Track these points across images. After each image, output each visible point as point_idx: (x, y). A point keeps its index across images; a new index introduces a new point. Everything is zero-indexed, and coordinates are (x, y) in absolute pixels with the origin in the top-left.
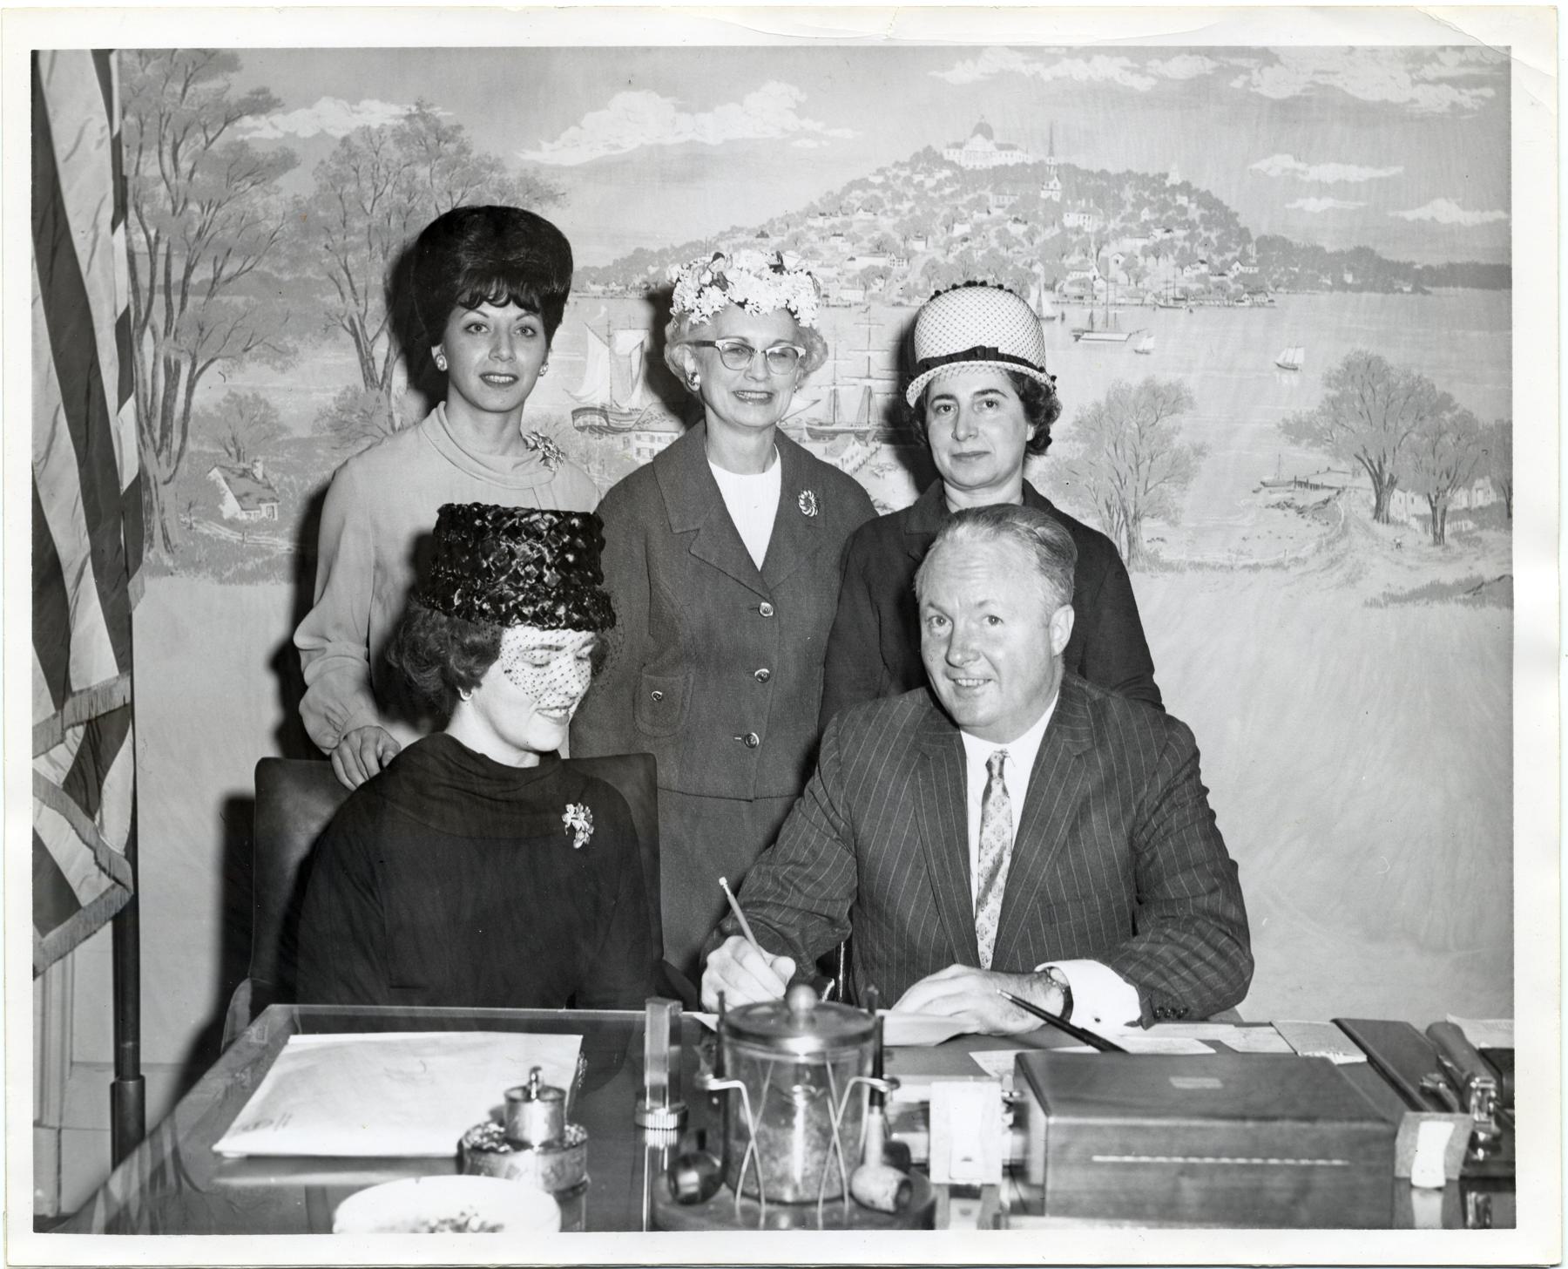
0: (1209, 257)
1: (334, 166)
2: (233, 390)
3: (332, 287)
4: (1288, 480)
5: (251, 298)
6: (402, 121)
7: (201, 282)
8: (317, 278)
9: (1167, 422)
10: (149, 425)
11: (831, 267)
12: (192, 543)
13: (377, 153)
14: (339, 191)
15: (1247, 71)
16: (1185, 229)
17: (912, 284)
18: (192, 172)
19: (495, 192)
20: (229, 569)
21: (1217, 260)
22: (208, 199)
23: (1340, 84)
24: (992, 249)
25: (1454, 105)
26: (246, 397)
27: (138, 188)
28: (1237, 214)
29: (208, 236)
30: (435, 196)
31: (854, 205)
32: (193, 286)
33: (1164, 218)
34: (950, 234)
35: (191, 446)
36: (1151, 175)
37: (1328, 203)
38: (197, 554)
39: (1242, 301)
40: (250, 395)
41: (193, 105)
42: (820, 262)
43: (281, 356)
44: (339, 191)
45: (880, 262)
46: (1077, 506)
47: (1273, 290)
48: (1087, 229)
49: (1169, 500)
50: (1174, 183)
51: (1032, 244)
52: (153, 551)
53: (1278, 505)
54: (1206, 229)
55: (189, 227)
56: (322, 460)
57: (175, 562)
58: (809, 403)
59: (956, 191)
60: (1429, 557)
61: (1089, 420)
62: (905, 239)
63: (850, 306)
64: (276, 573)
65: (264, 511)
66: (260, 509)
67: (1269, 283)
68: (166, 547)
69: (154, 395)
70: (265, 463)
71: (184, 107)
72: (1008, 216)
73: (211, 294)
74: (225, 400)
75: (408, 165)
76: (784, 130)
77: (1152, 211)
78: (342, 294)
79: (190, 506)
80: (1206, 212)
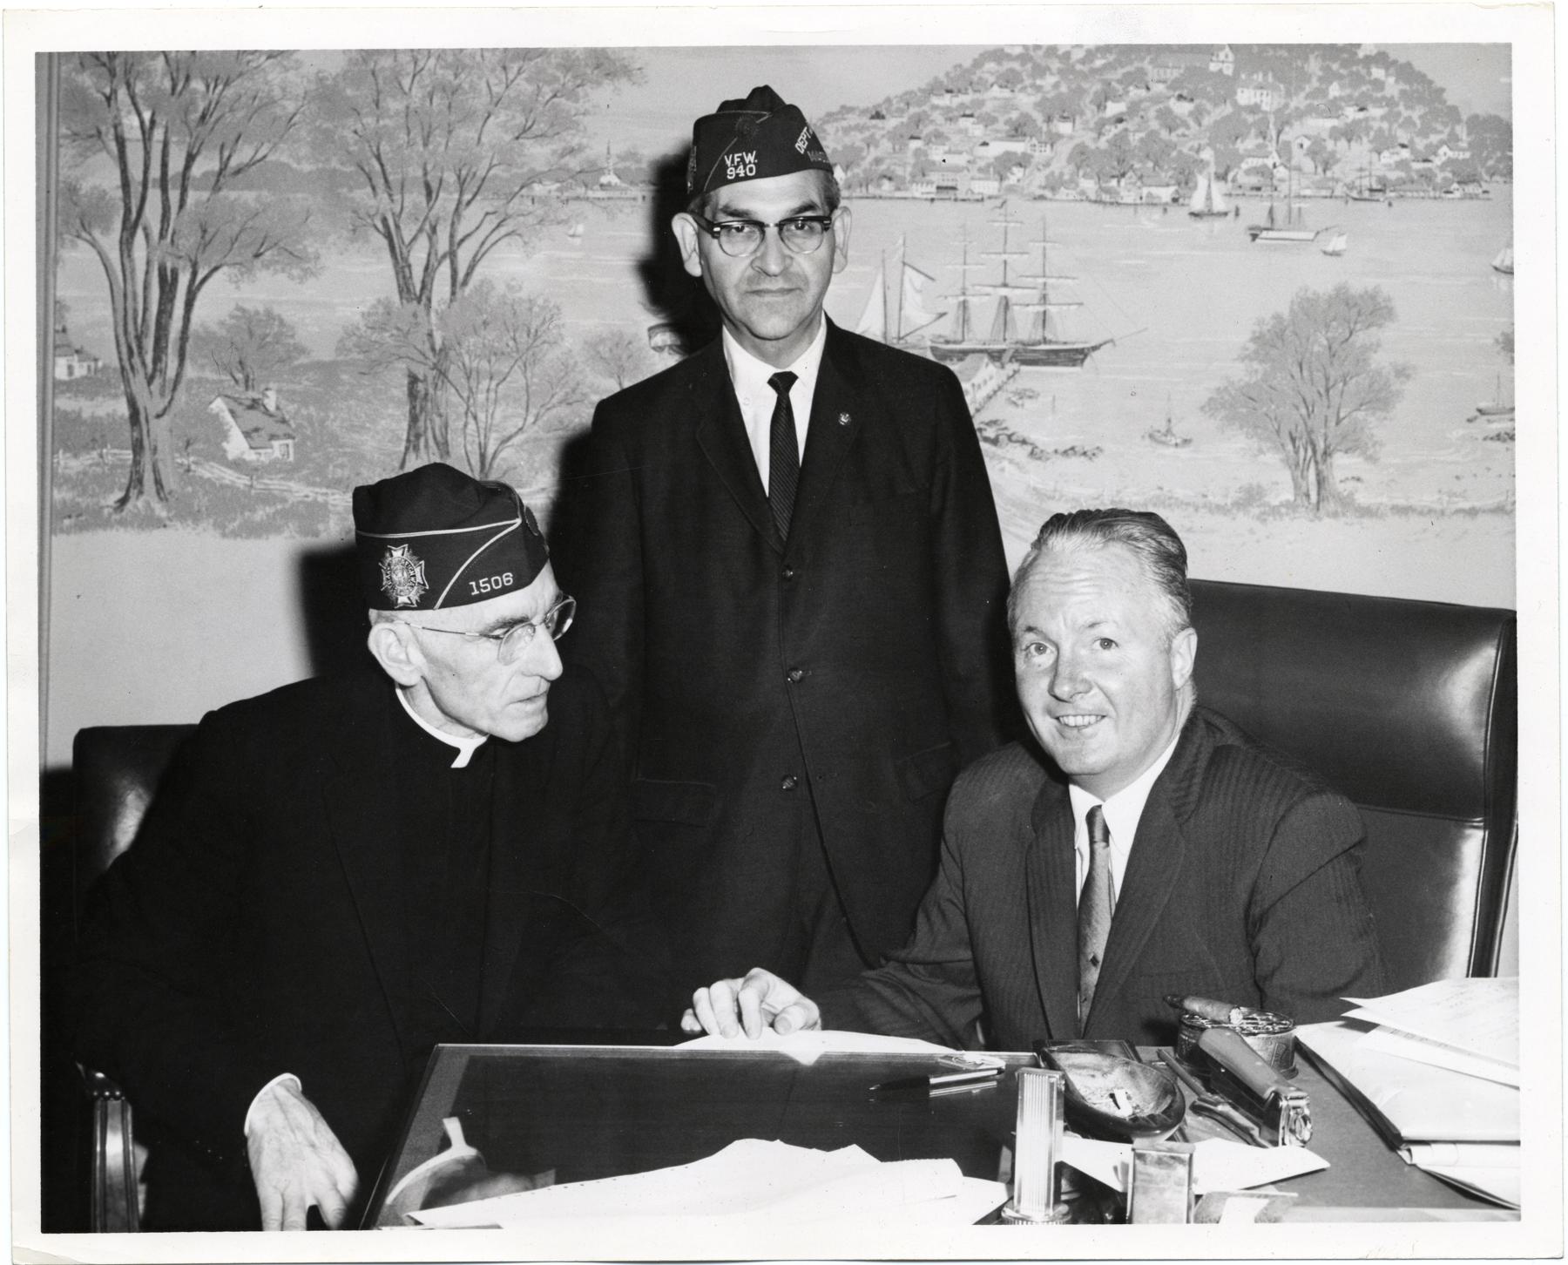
0: (1412, 141)
2: (240, 304)
3: (362, 180)
5: (265, 193)
7: (205, 175)
8: (345, 169)
9: (1361, 338)
10: (140, 347)
11: (960, 153)
12: (190, 489)
14: (372, 64)
16: (1382, 107)
17: (1057, 174)
19: (559, 66)
20: (235, 520)
21: (1420, 144)
22: (214, 74)
24: (1152, 131)
26: (257, 313)
27: (130, 62)
28: (1442, 90)
29: (213, 119)
30: (487, 73)
31: (987, 81)
32: (195, 179)
33: (1356, 94)
34: (1101, 115)
35: (190, 372)
38: (196, 502)
39: (1451, 192)
40: (261, 309)
42: (946, 148)
43: (296, 260)
44: (372, 65)
45: (1018, 147)
46: (1255, 439)
47: (1486, 177)
48: (1265, 107)
49: (1367, 431)
50: (1368, 53)
51: (1200, 125)
52: (142, 498)
53: (1498, 437)
54: (1407, 107)
55: (191, 108)
56: (348, 387)
57: (169, 511)
58: (934, 316)
59: (1110, 63)
61: (1268, 336)
62: (1049, 120)
63: (982, 200)
64: (290, 525)
66: (272, 447)
67: (1483, 171)
68: (158, 494)
69: (145, 310)
70: (279, 391)
72: (1171, 93)
73: (216, 188)
74: (232, 317)
77: (1342, 87)
78: (374, 188)
79: (188, 444)
80: (1407, 87)
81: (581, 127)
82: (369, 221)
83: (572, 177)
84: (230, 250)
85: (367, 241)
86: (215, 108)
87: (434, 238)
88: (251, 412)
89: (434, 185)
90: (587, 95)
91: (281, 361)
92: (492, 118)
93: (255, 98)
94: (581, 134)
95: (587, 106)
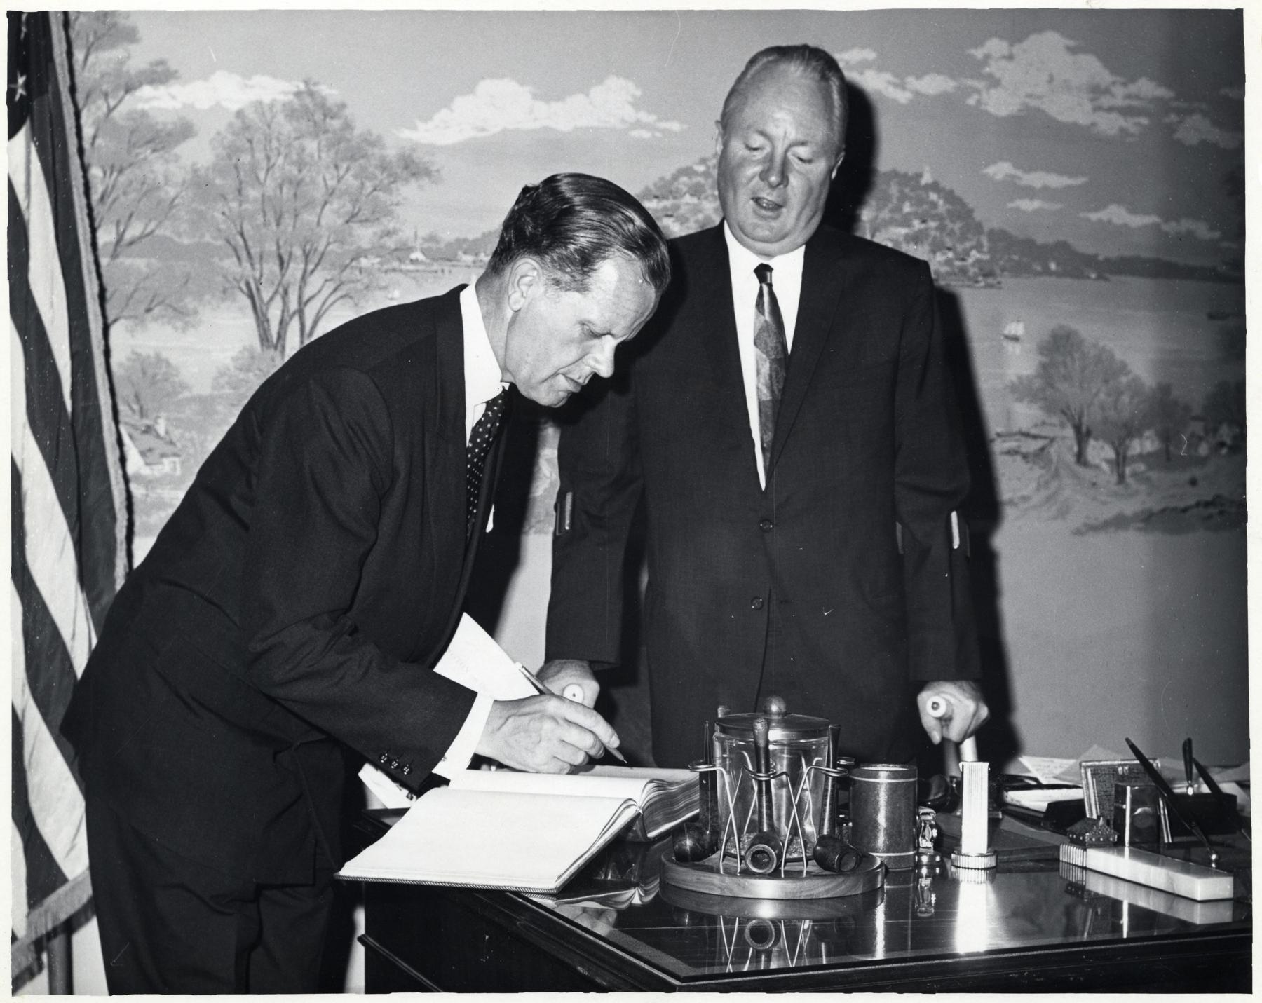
0: (954, 246)
1: (230, 137)
4: (1015, 429)
5: (153, 261)
6: (291, 97)
8: (214, 242)
13: (269, 126)
15: (978, 91)
18: (94, 138)
19: (376, 167)
21: (960, 248)
23: (1043, 107)
25: (1122, 130)
26: (149, 357)
29: (110, 200)
31: (682, 190)
33: (920, 211)
36: (910, 174)
37: (1036, 204)
40: (152, 354)
41: (94, 72)
43: (181, 315)
44: (234, 161)
54: (952, 222)
60: (1116, 494)
65: (167, 466)
66: (162, 463)
70: (168, 419)
71: (86, 74)
74: (129, 359)
75: (297, 138)
76: (623, 121)
77: (912, 205)
78: (239, 259)
81: (395, 215)
82: (235, 283)
83: (389, 254)
84: (127, 305)
85: (234, 300)
86: (111, 192)
87: (286, 299)
88: (146, 437)
89: (286, 257)
90: (398, 190)
91: (168, 395)
92: (328, 207)
93: (143, 183)
94: (394, 221)
95: (400, 198)
